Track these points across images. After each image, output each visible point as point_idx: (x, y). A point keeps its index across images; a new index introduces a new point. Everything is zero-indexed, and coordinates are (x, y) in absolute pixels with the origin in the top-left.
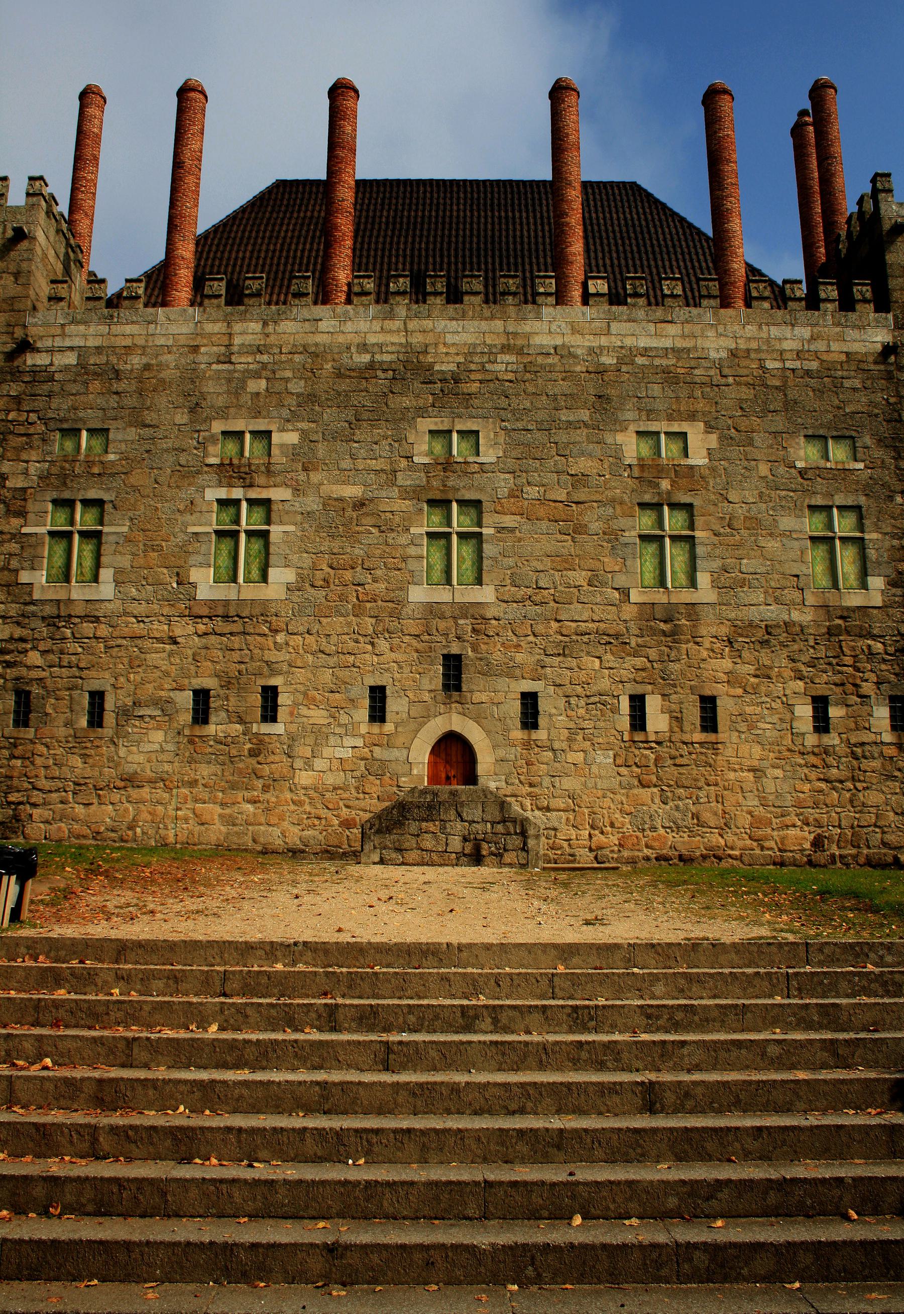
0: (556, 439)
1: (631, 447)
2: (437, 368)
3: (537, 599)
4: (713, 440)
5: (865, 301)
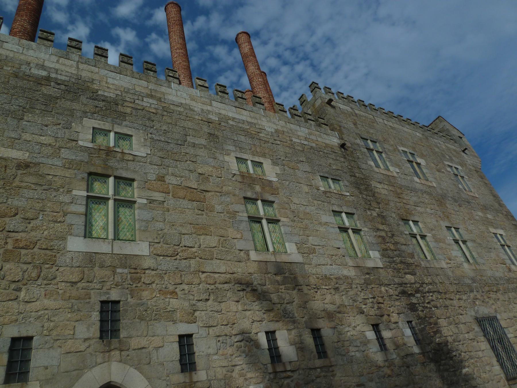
0: (188, 151)
2: (99, 93)
3: (185, 255)
4: (278, 170)
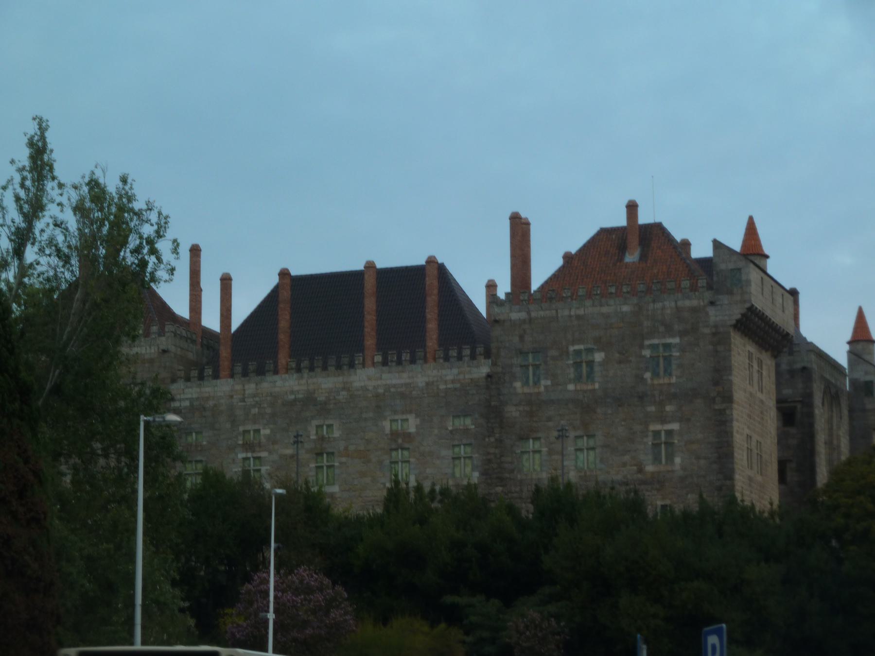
1: (387, 425)
5: (480, 354)
